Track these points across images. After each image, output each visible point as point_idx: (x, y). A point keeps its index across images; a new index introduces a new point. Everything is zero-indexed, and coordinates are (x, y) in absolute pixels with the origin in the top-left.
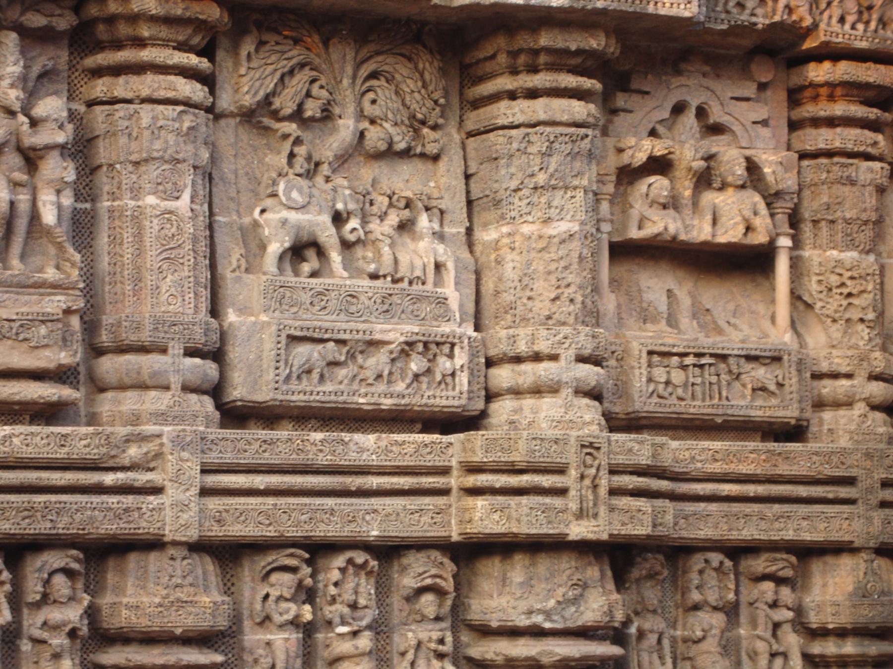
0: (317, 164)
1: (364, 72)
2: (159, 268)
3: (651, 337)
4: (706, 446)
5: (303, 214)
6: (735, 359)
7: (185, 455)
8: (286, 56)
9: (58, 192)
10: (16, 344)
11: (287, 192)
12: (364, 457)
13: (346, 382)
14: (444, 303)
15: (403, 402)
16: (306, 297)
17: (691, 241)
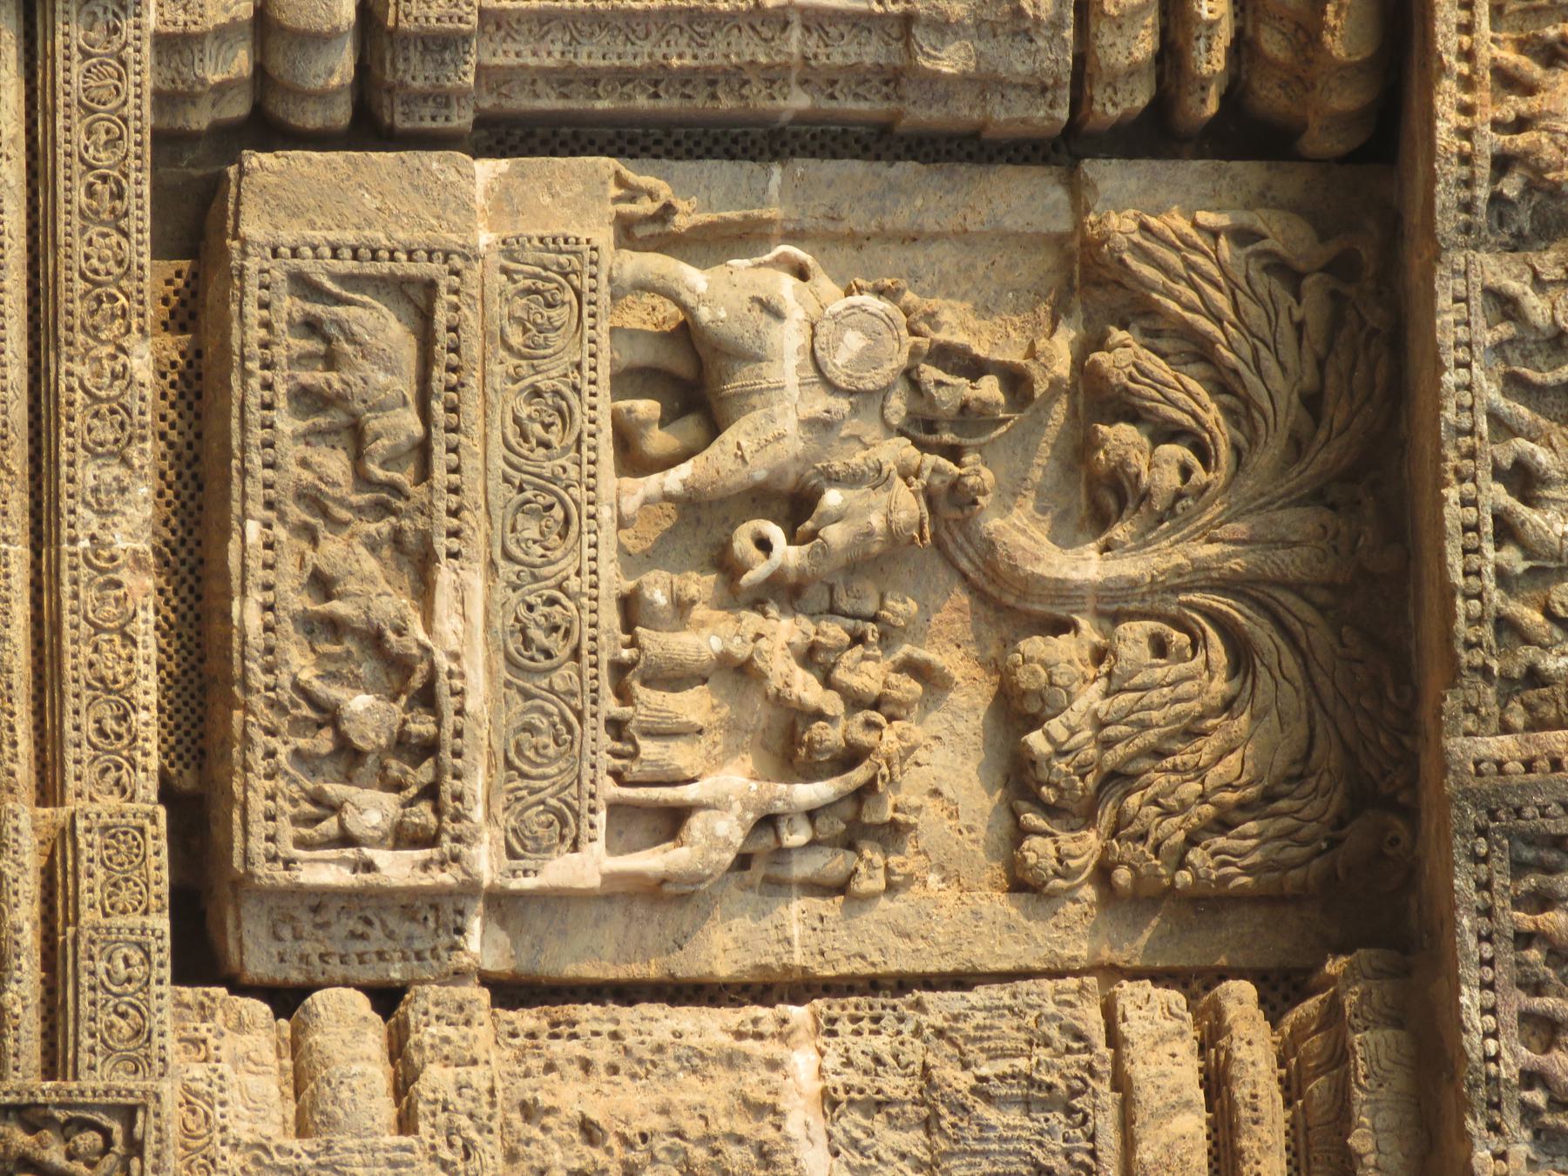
0: (954, 453)
5: (800, 368)
8: (1264, 352)
13: (307, 476)
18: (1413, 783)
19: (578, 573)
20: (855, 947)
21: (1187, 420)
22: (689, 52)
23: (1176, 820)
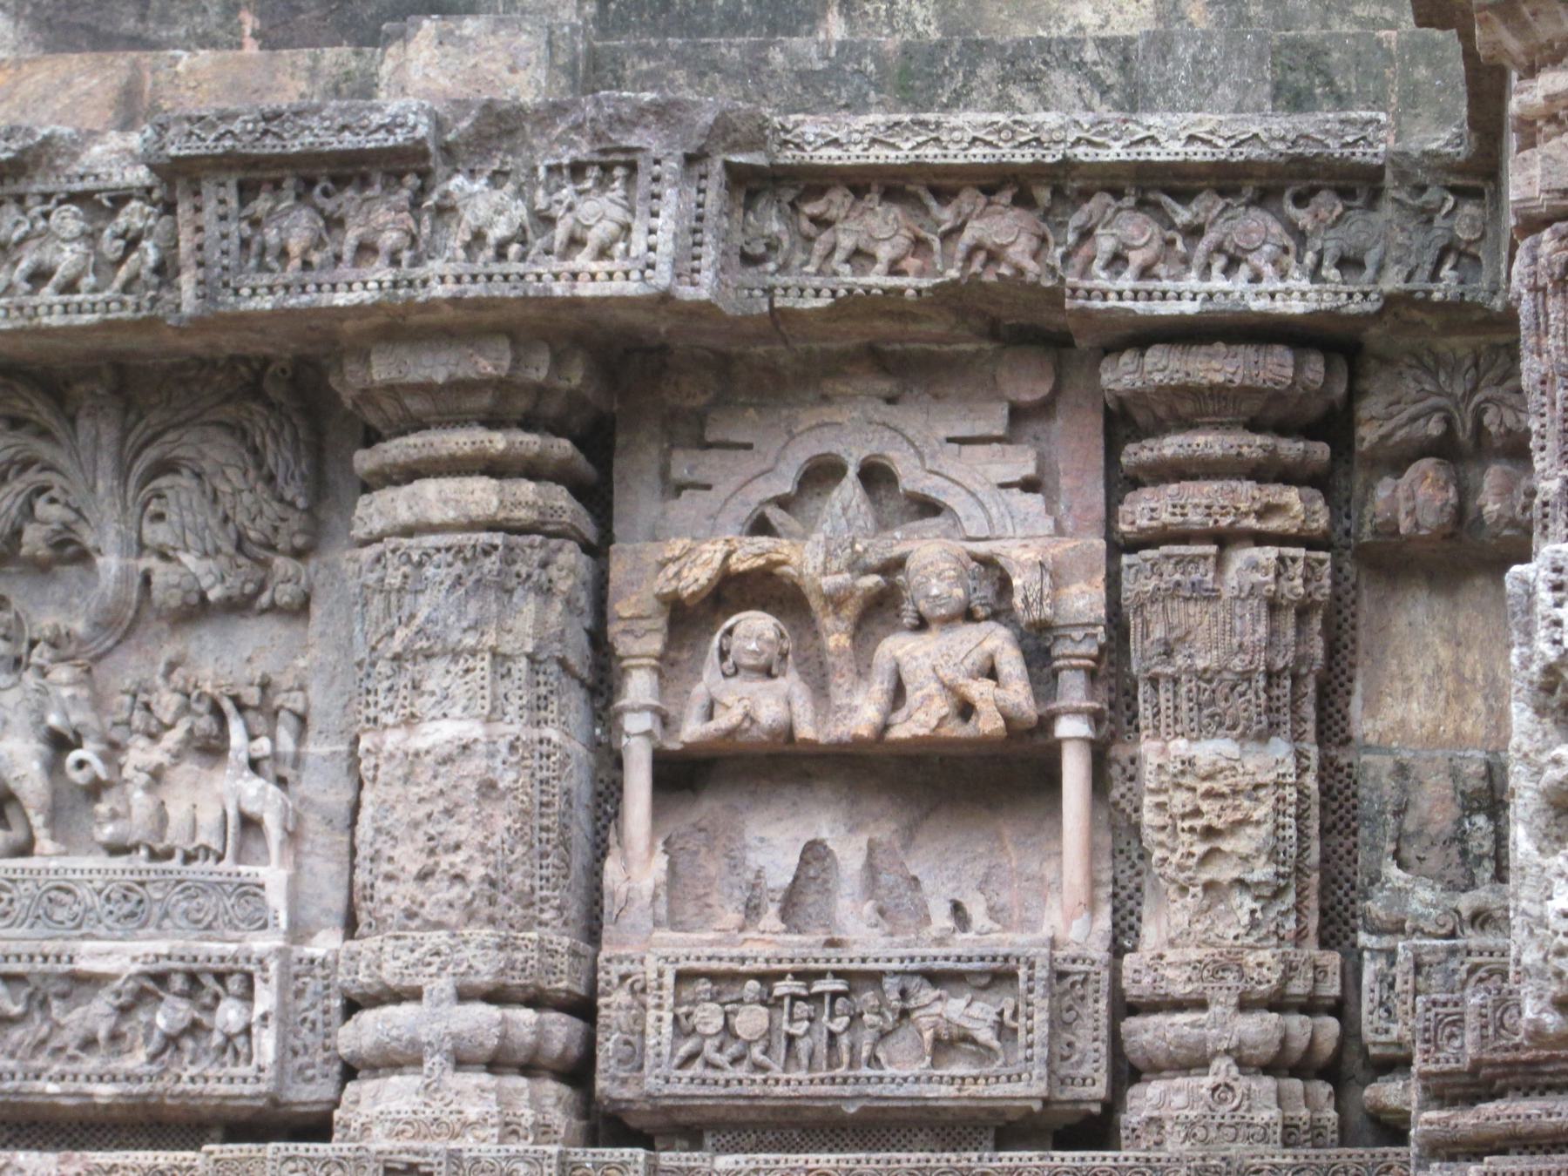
1: (139, 467)
3: (711, 943)
4: (801, 1163)
6: (896, 980)
14: (255, 895)
15: (136, 1089)
17: (846, 738)
18: (246, 360)
19: (91, 882)
20: (338, 712)
21: (20, 500)
23: (265, 507)
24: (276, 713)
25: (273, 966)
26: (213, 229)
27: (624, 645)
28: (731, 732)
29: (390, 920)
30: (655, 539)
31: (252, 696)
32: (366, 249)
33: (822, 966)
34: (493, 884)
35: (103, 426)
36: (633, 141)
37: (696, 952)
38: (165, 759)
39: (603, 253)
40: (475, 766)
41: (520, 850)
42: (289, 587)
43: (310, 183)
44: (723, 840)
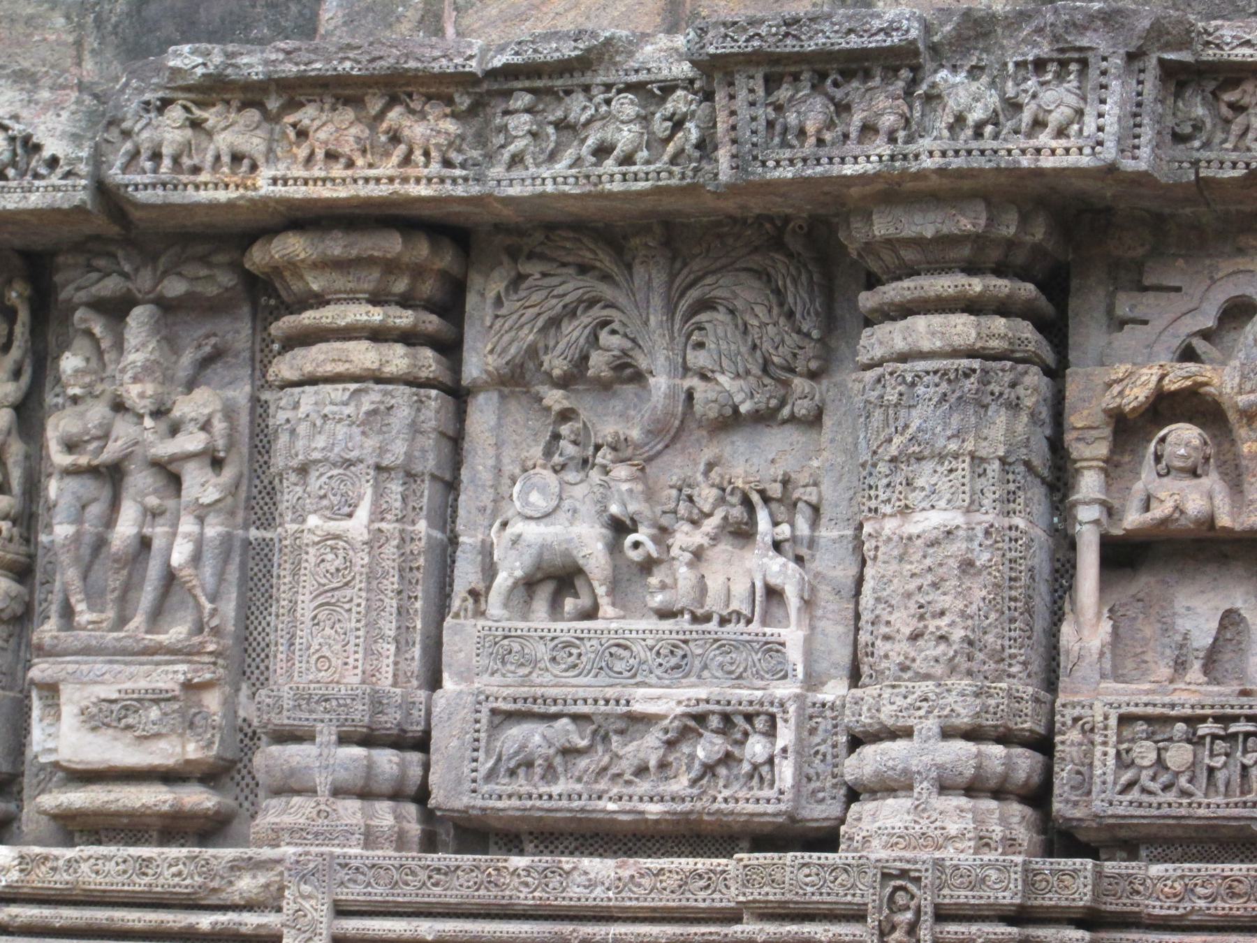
1: (684, 305)
2: (315, 617)
3: (1147, 692)
4: (1218, 871)
5: (546, 525)
7: (306, 889)
8: (555, 293)
9: (201, 520)
10: (119, 734)
11: (525, 493)
12: (598, 891)
14: (778, 651)
15: (679, 807)
16: (542, 651)
18: (770, 219)
20: (845, 503)
21: (587, 331)
22: (392, 579)
23: (786, 337)
24: (795, 505)
25: (792, 709)
26: (744, 113)
27: (1078, 450)
28: (1164, 521)
29: (887, 672)
30: (1102, 364)
31: (775, 490)
32: (868, 129)
33: (1237, 711)
34: (971, 643)
35: (654, 272)
36: (1084, 42)
37: (1135, 699)
38: (705, 541)
39: (1061, 133)
40: (957, 548)
41: (993, 616)
42: (806, 402)
43: (823, 76)
44: (1157, 608)
